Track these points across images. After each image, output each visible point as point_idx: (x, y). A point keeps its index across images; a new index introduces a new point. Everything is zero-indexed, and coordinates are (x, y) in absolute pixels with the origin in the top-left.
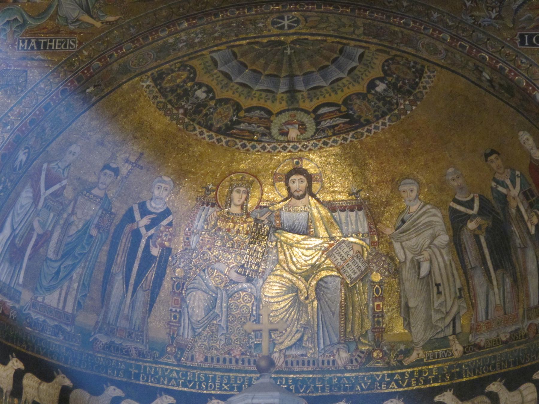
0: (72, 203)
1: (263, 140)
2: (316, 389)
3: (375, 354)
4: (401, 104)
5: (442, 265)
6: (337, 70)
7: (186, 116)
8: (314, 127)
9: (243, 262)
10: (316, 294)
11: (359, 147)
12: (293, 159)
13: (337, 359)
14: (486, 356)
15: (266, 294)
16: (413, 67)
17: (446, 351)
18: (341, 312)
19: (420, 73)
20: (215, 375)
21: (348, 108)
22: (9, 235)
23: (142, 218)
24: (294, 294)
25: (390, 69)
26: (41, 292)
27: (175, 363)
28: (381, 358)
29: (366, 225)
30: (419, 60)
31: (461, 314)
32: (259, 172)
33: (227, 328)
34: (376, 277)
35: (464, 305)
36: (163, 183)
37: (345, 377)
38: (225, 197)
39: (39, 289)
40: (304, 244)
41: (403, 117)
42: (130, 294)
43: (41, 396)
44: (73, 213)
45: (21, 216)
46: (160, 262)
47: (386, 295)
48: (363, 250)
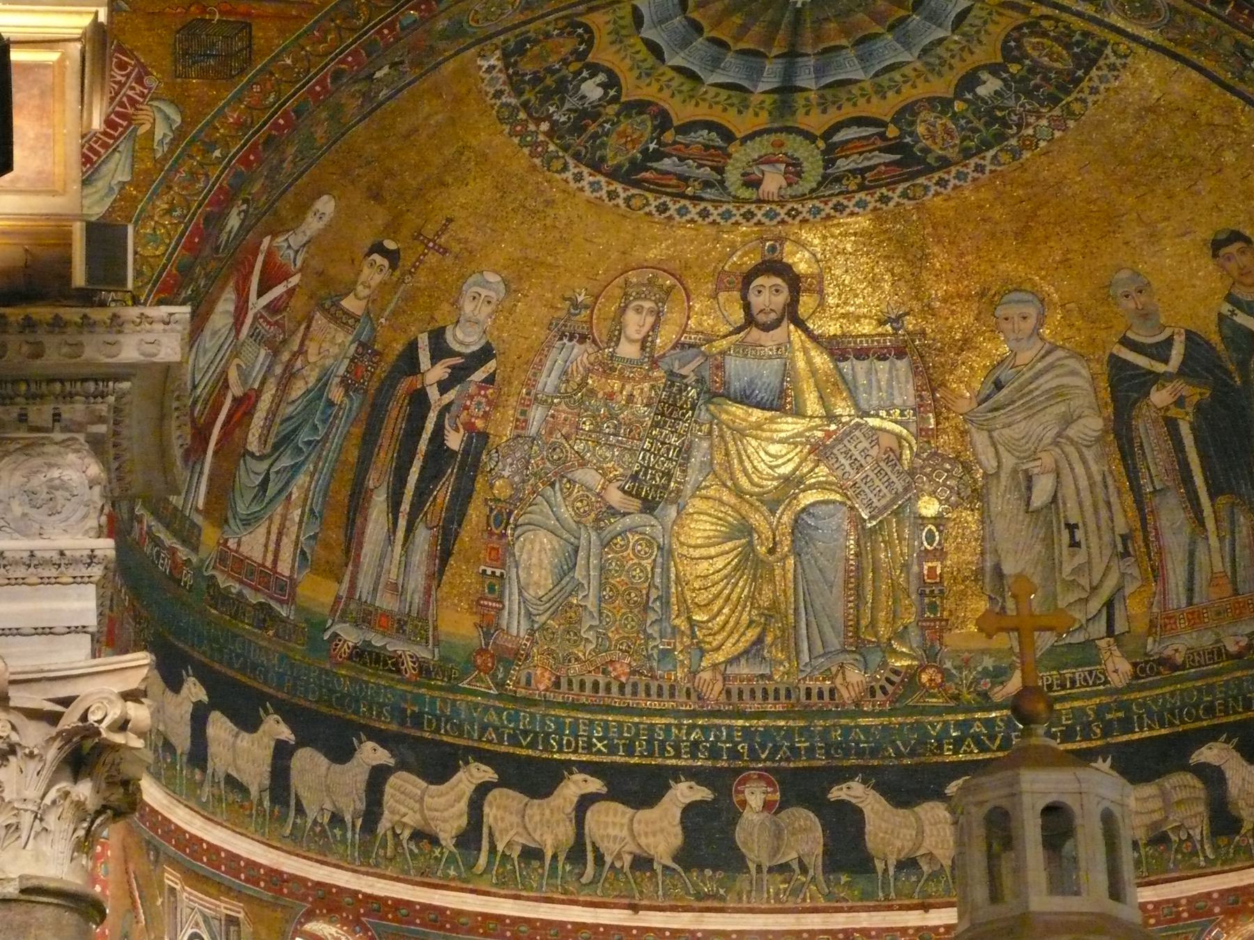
0: (303, 327)
1: (704, 195)
2: (795, 751)
4: (1028, 125)
5: (1083, 483)
6: (898, 46)
7: (551, 138)
8: (821, 171)
10: (793, 541)
11: (915, 217)
12: (763, 240)
13: (839, 687)
14: (1189, 685)
15: (682, 539)
16: (1078, 44)
17: (1090, 673)
18: (846, 582)
19: (1088, 59)
20: (577, 719)
21: (900, 129)
23: (433, 364)
24: (743, 541)
25: (1019, 46)
27: (494, 692)
28: (940, 685)
30: (1095, 29)
31: (1128, 591)
32: (687, 267)
33: (600, 613)
34: (929, 507)
35: (1136, 572)
36: (484, 287)
37: (857, 726)
38: (609, 323)
39: (231, 521)
40: (771, 431)
41: (1027, 155)
42: (400, 534)
43: (239, 762)
45: (210, 355)
47: (949, 546)
48: (901, 447)
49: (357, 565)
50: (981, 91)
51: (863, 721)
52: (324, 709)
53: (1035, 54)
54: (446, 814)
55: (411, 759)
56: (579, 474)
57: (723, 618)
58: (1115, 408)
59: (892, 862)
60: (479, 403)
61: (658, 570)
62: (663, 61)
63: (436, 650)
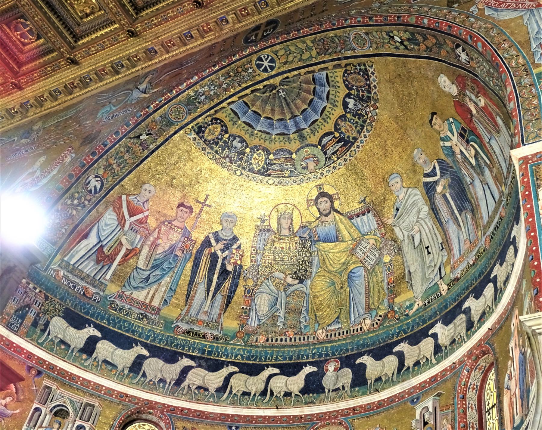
0: (157, 230)
2: (347, 350)
3: (389, 315)
5: (427, 231)
8: (324, 157)
9: (295, 270)
15: (313, 290)
16: (360, 69)
20: (273, 351)
21: (339, 133)
26: (130, 289)
29: (375, 223)
33: (285, 317)
34: (387, 259)
41: (374, 124)
44: (158, 238)
46: (234, 276)
50: (351, 106)
51: (369, 336)
52: (167, 347)
53: (354, 83)
54: (214, 382)
55: (204, 364)
56: (277, 274)
58: (430, 201)
59: (373, 380)
60: (237, 256)
61: (305, 301)
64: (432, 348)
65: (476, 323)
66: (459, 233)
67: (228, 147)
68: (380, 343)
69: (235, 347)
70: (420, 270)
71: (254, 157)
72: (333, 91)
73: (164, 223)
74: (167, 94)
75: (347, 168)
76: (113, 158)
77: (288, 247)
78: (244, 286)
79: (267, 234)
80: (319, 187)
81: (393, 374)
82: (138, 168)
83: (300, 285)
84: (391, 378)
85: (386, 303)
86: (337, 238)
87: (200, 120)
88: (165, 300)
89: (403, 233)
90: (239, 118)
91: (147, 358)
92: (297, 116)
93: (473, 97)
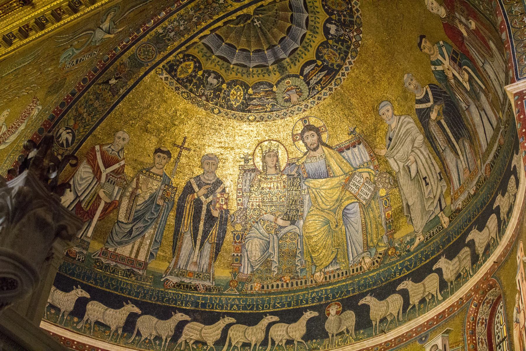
0: (135, 180)
2: (348, 292)
3: (390, 252)
5: (424, 160)
8: (307, 87)
9: (286, 211)
15: (306, 231)
18: (362, 229)
20: (270, 298)
21: (321, 61)
22: (73, 199)
29: (367, 155)
33: (279, 261)
34: (382, 192)
41: (359, 49)
42: (198, 247)
44: (137, 187)
46: (221, 222)
49: (178, 257)
50: (332, 32)
51: (371, 275)
52: (159, 303)
53: (334, 7)
54: (211, 335)
57: (323, 253)
60: (222, 200)
61: (299, 243)
62: (231, 64)
63: (214, 282)
64: (437, 284)
65: (481, 256)
66: (457, 162)
67: (203, 84)
68: (382, 282)
69: (229, 297)
70: (419, 203)
71: (231, 93)
72: (311, 17)
73: (142, 172)
74: (133, 34)
75: (333, 98)
76: (83, 107)
77: (275, 187)
78: (232, 232)
79: (253, 174)
80: (304, 120)
81: (398, 314)
82: (110, 115)
83: (292, 227)
84: (396, 317)
85: (385, 240)
86: (328, 174)
87: (171, 58)
88: (151, 253)
89: (398, 164)
90: (212, 52)
91: (139, 316)
92: (275, 46)
93: (463, 20)
